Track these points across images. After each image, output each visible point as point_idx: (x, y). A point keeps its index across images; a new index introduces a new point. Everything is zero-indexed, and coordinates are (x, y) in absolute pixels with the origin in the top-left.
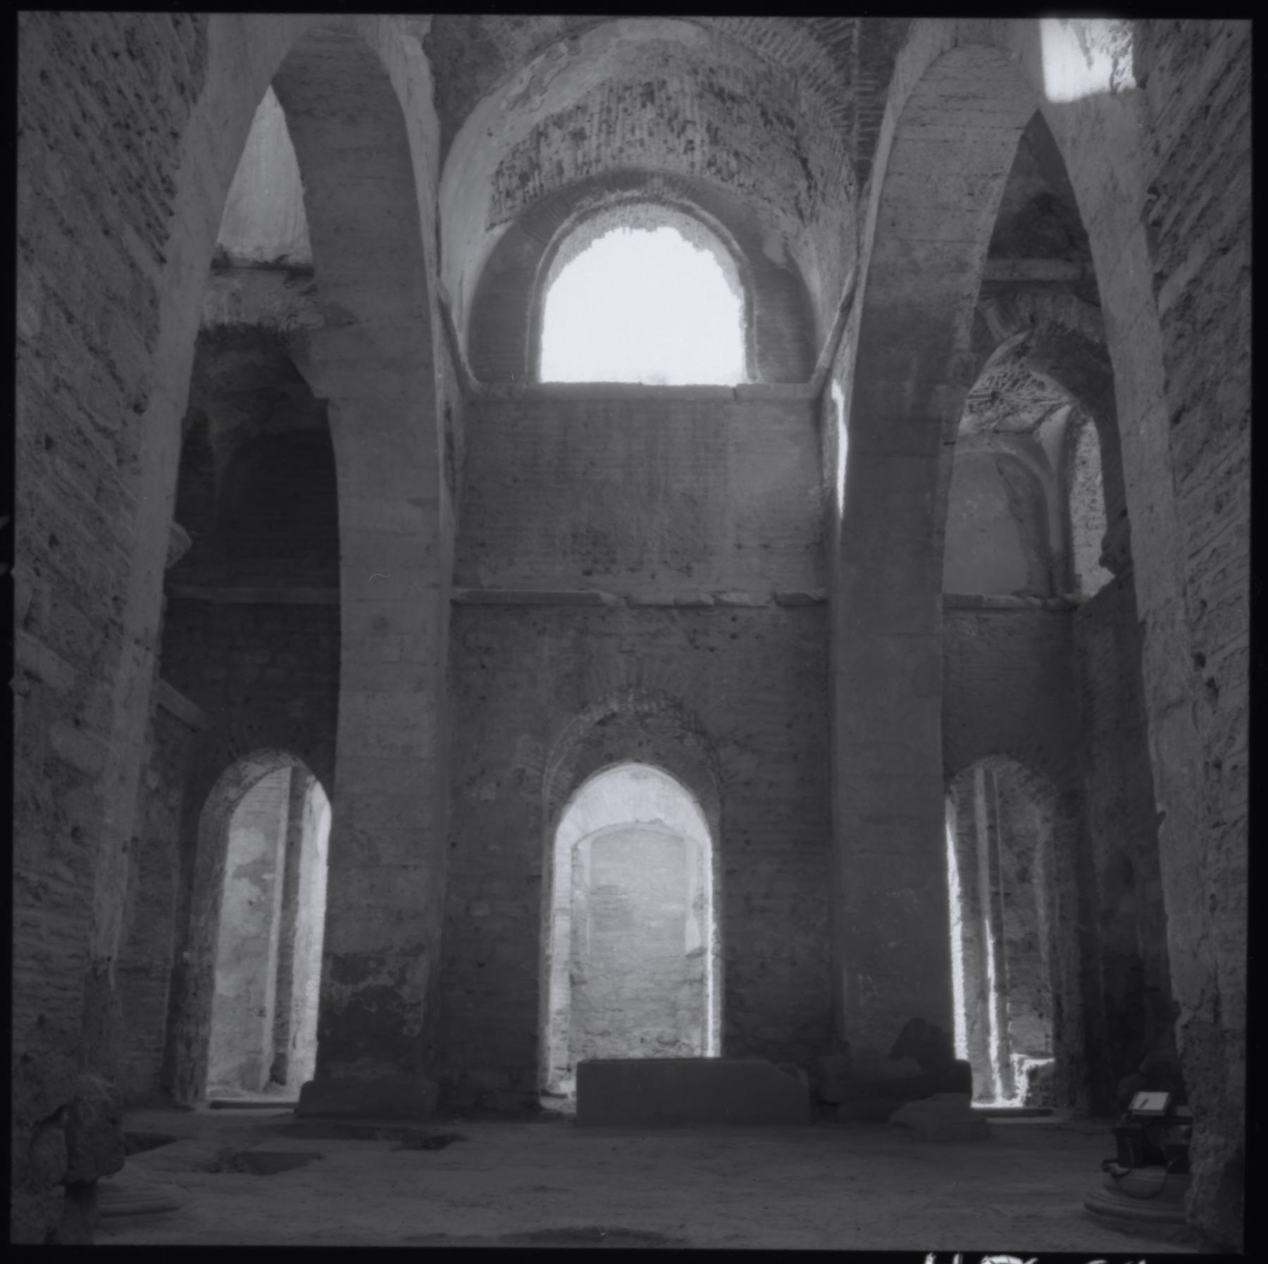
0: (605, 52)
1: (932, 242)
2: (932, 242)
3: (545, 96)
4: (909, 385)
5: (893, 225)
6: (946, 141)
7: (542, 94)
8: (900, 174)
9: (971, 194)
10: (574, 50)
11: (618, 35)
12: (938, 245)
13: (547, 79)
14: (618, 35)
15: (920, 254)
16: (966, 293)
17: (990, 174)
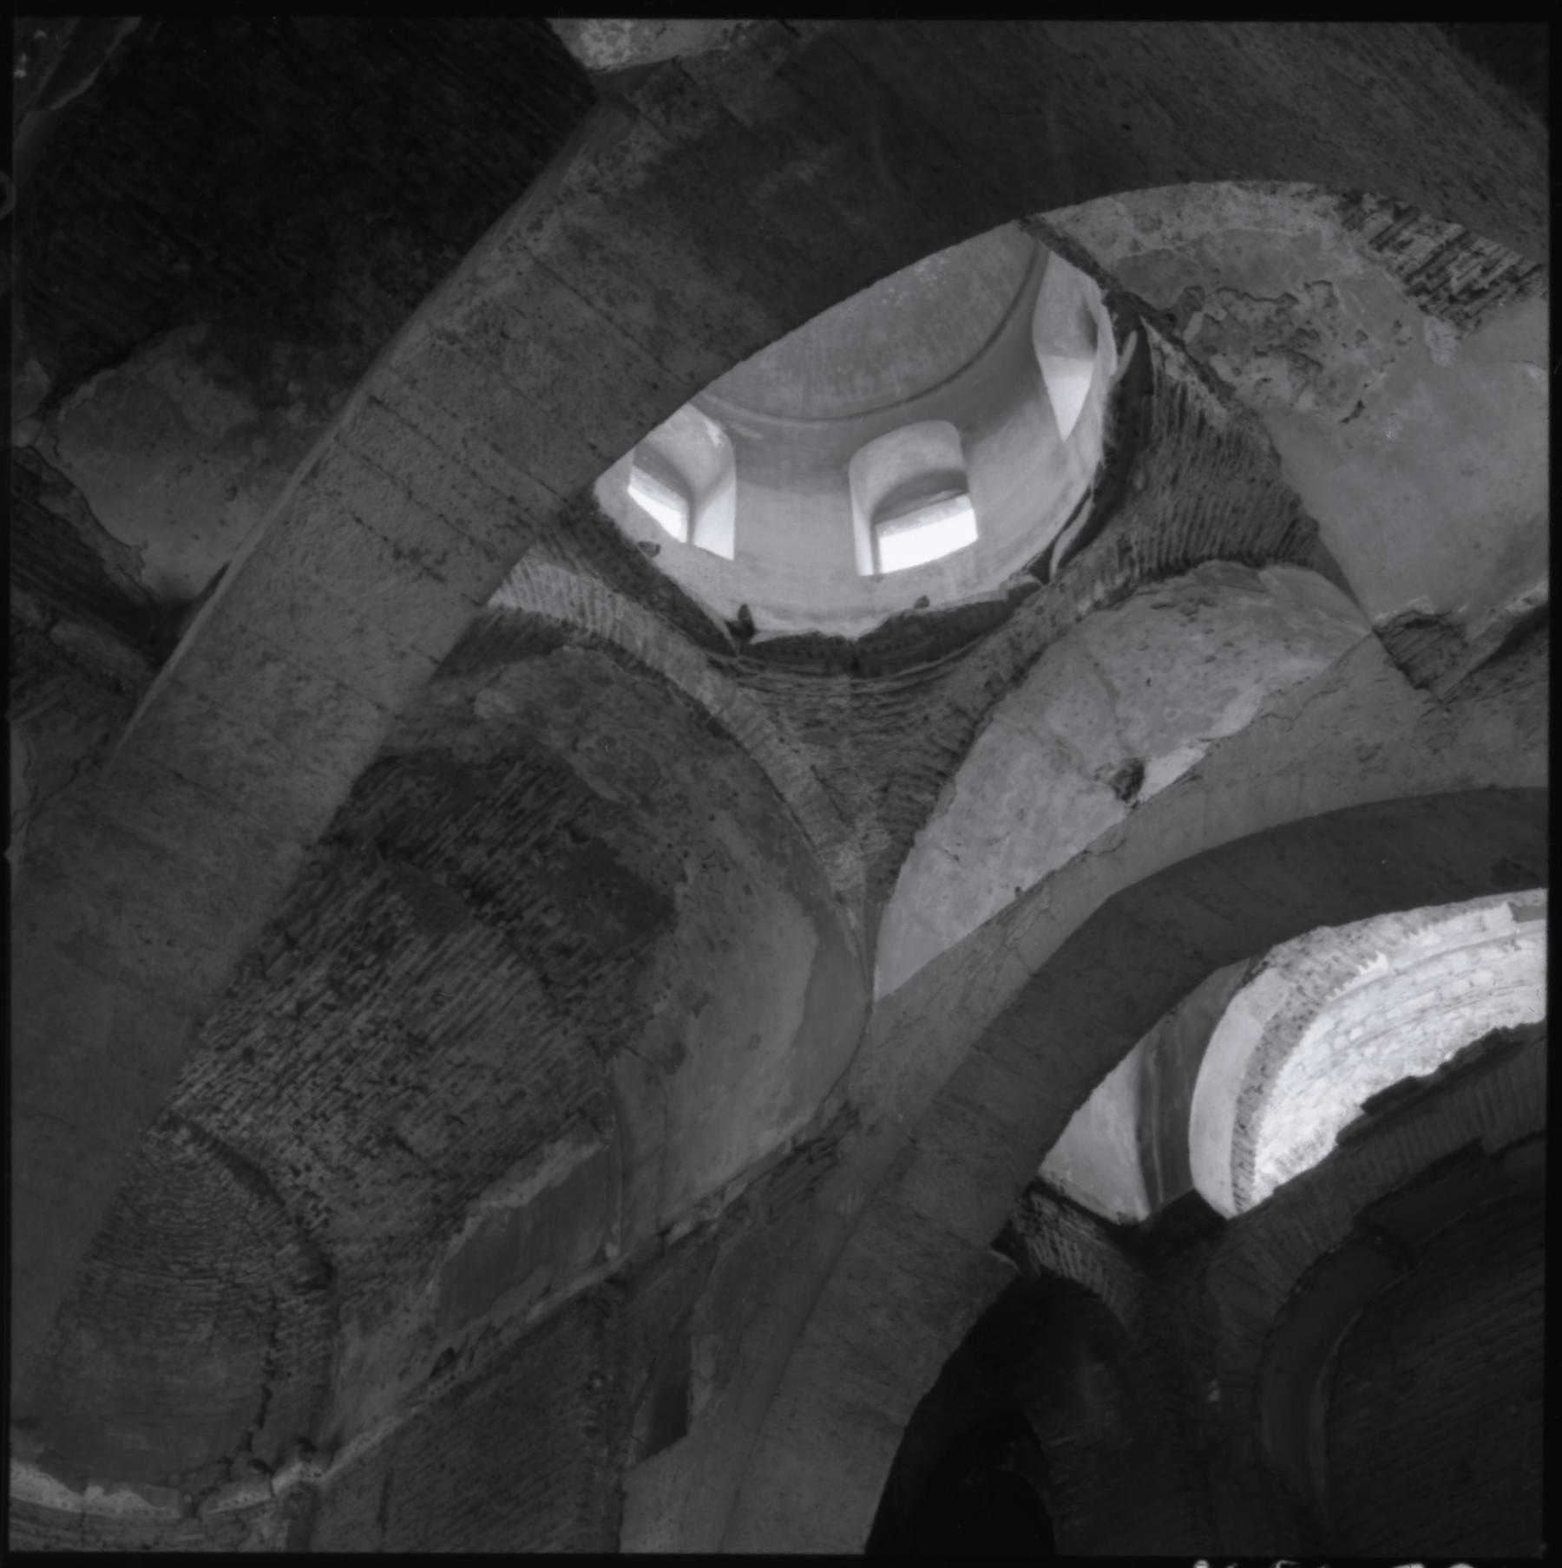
0: (1179, 237)
1: (609, 318)
2: (609, 318)
3: (1296, 289)
4: (805, 172)
5: (655, 386)
6: (494, 446)
7: (1295, 300)
8: (594, 448)
9: (504, 335)
10: (1192, 302)
11: (1136, 245)
12: (601, 303)
13: (1262, 311)
14: (1136, 245)
15: (641, 314)
16: (596, 198)
17: (456, 348)
